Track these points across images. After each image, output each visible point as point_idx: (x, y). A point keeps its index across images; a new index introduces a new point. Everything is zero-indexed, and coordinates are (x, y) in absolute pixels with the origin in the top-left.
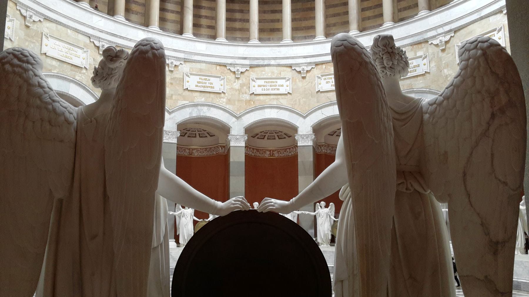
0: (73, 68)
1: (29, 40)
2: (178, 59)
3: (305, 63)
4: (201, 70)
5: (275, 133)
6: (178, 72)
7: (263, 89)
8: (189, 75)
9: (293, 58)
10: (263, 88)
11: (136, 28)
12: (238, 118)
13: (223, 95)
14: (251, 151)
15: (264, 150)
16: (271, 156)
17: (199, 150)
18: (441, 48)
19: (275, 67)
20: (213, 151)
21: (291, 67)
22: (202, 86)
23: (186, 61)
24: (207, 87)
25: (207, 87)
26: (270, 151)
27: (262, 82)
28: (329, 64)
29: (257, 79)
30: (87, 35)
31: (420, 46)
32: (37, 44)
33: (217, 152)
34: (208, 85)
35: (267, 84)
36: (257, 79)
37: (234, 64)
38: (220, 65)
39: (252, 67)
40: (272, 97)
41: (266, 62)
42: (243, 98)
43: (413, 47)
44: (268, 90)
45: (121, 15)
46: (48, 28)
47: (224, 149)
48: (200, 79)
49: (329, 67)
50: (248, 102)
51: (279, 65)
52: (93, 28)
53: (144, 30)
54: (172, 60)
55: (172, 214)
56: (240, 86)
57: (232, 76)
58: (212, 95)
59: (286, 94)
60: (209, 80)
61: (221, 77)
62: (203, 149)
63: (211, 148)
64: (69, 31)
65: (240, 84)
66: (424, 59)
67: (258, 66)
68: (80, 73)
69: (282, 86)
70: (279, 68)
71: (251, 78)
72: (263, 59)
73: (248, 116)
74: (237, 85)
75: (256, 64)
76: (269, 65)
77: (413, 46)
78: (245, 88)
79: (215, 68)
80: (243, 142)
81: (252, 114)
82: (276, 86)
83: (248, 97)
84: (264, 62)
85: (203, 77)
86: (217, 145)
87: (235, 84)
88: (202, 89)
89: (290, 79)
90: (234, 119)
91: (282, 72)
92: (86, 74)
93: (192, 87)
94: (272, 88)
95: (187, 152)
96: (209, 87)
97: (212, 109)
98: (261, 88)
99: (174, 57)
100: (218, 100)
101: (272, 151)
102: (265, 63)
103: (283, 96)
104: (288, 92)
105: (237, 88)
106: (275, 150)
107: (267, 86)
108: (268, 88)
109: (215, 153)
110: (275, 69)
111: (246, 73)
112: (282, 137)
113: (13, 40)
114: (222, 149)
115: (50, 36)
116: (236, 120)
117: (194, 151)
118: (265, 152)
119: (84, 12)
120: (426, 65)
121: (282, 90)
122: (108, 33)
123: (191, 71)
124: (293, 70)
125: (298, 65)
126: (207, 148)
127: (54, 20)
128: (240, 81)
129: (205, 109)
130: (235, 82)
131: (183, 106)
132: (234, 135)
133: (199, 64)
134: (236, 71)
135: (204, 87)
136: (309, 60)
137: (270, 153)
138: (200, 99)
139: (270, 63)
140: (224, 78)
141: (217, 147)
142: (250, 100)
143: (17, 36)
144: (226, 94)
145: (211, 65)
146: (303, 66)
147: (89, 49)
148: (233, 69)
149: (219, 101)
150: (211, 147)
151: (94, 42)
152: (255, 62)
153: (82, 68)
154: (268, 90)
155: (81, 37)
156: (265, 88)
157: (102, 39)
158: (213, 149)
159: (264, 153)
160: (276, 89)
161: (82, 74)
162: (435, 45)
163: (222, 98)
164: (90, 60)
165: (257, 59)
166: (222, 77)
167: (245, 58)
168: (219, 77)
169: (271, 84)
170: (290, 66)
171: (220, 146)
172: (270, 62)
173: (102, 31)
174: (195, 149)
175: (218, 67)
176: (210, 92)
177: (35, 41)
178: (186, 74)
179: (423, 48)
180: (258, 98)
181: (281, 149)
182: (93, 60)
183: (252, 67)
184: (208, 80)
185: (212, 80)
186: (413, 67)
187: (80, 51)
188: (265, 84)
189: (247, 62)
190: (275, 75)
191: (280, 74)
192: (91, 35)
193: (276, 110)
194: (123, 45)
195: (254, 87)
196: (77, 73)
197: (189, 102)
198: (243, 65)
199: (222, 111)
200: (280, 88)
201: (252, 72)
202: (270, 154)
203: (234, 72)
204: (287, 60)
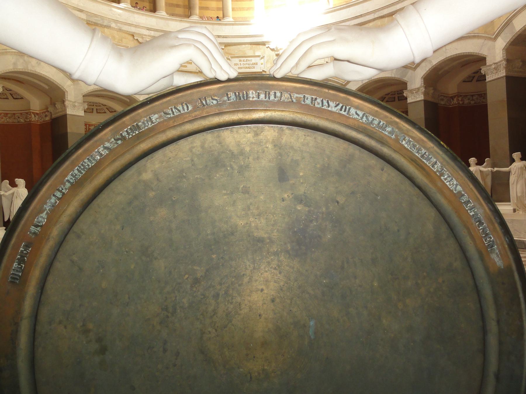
18: (276, 53)
20: (19, 118)
21: (133, 36)
31: (258, 46)
41: (105, 23)
43: (252, 47)
47: (37, 117)
51: (120, 30)
63: (14, 114)
66: (261, 58)
72: (102, 18)
75: (94, 21)
76: (108, 27)
77: (252, 45)
80: (82, 111)
90: (69, 82)
91: (123, 40)
101: (87, 125)
102: (105, 24)
109: (22, 120)
112: (101, 112)
114: (35, 116)
120: (263, 65)
126: (7, 114)
139: (111, 25)
141: (27, 113)
152: (93, 19)
158: (19, 116)
162: (271, 49)
167: (81, 11)
171: (33, 113)
172: (110, 24)
179: (260, 49)
186: (252, 64)
190: (116, 40)
204: (129, 27)
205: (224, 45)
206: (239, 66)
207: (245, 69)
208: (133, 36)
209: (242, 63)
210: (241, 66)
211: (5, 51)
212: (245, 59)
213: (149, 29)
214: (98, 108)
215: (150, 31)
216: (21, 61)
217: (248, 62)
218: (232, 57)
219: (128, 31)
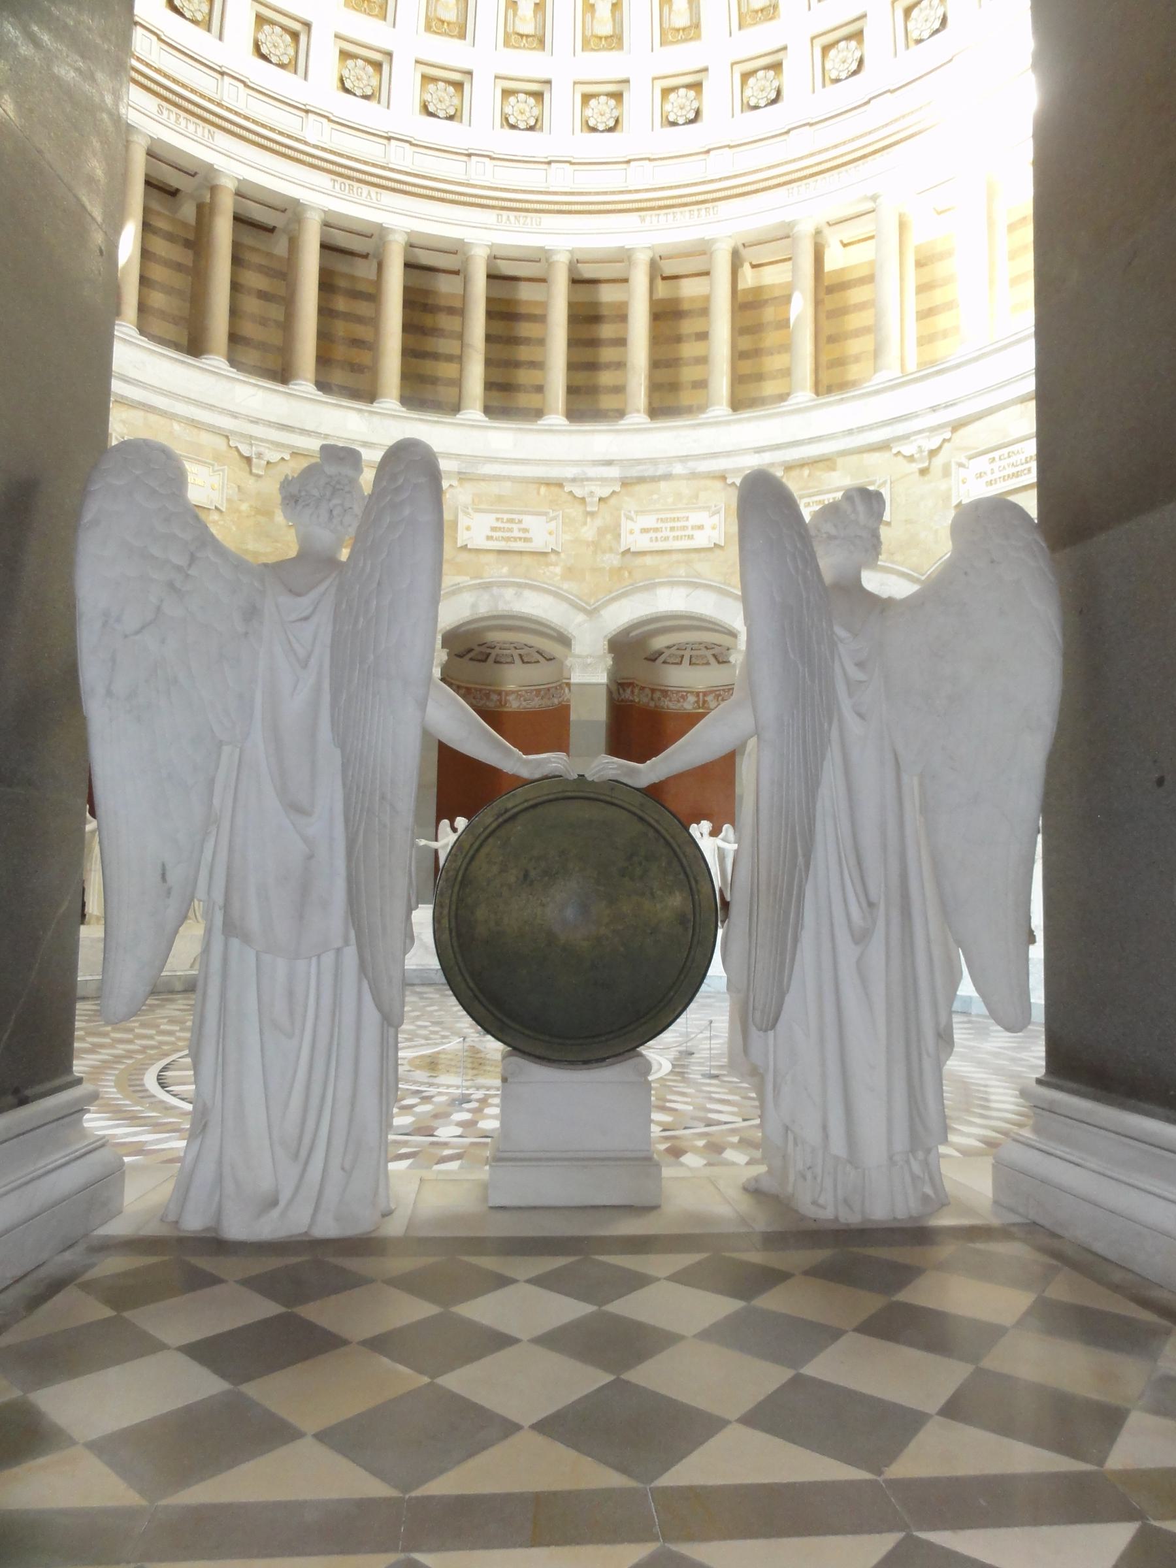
4: (500, 499)
5: (704, 649)
7: (654, 539)
10: (653, 535)
11: (341, 406)
12: (592, 613)
13: (553, 557)
14: (647, 695)
15: (682, 691)
16: (699, 708)
17: (521, 696)
21: (724, 478)
22: (502, 537)
24: (515, 539)
25: (515, 539)
26: (698, 694)
27: (649, 521)
28: (821, 465)
30: (221, 432)
33: (561, 699)
34: (516, 534)
37: (582, 480)
38: (548, 483)
39: (625, 483)
40: (675, 557)
44: (666, 539)
45: (306, 380)
46: (124, 422)
48: (498, 519)
49: (818, 473)
50: (616, 572)
51: (694, 476)
52: (234, 415)
53: (360, 410)
55: (425, 846)
57: (575, 511)
58: (527, 560)
59: (710, 549)
61: (548, 513)
62: (532, 691)
63: (548, 689)
64: (176, 426)
67: (641, 480)
69: (701, 527)
71: (622, 512)
72: (654, 462)
73: (614, 607)
75: (636, 475)
76: (667, 477)
78: (609, 537)
81: (624, 602)
82: (684, 528)
83: (615, 560)
85: (506, 517)
86: (558, 683)
87: (584, 529)
88: (501, 545)
89: (721, 508)
90: (581, 617)
93: (479, 541)
94: (675, 534)
95: (495, 699)
96: (520, 539)
97: (527, 593)
98: (647, 536)
100: (541, 571)
101: (701, 695)
102: (659, 473)
103: (703, 555)
104: (715, 544)
105: (590, 539)
106: (711, 692)
107: (664, 529)
108: (664, 534)
111: (613, 501)
116: (588, 619)
117: (511, 698)
118: (684, 698)
119: (212, 379)
121: (702, 540)
122: (270, 424)
126: (538, 691)
127: (140, 403)
128: (598, 522)
129: (509, 593)
130: (585, 523)
131: (454, 587)
132: (579, 657)
135: (508, 539)
137: (696, 699)
138: (499, 570)
140: (558, 516)
141: (560, 685)
142: (620, 569)
144: (563, 556)
147: (224, 465)
148: (579, 492)
149: (544, 573)
150: (549, 686)
151: (239, 447)
152: (634, 472)
153: (209, 509)
154: (666, 539)
155: (205, 438)
156: (659, 535)
157: (256, 439)
159: (682, 700)
160: (685, 536)
163: (551, 565)
165: (639, 462)
166: (552, 514)
167: (609, 463)
168: (546, 514)
169: (672, 524)
172: (670, 469)
173: (256, 421)
174: (513, 692)
175: (543, 490)
176: (521, 553)
180: (639, 561)
181: (723, 690)
182: (237, 489)
184: (517, 521)
185: (528, 521)
186: (1023, 461)
188: (659, 525)
189: (614, 472)
191: (697, 497)
192: (232, 432)
193: (681, 591)
194: (308, 450)
195: (631, 532)
197: (471, 578)
198: (604, 480)
199: (550, 599)
200: (696, 533)
202: (697, 702)
205: (950, 429)
206: (989, 477)
207: (1004, 480)
208: (724, 478)
209: (995, 466)
210: (993, 477)
211: (457, 586)
212: (1005, 451)
214: (694, 653)
215: (763, 454)
216: (486, 597)
217: (1013, 460)
218: (970, 458)
219: (709, 472)
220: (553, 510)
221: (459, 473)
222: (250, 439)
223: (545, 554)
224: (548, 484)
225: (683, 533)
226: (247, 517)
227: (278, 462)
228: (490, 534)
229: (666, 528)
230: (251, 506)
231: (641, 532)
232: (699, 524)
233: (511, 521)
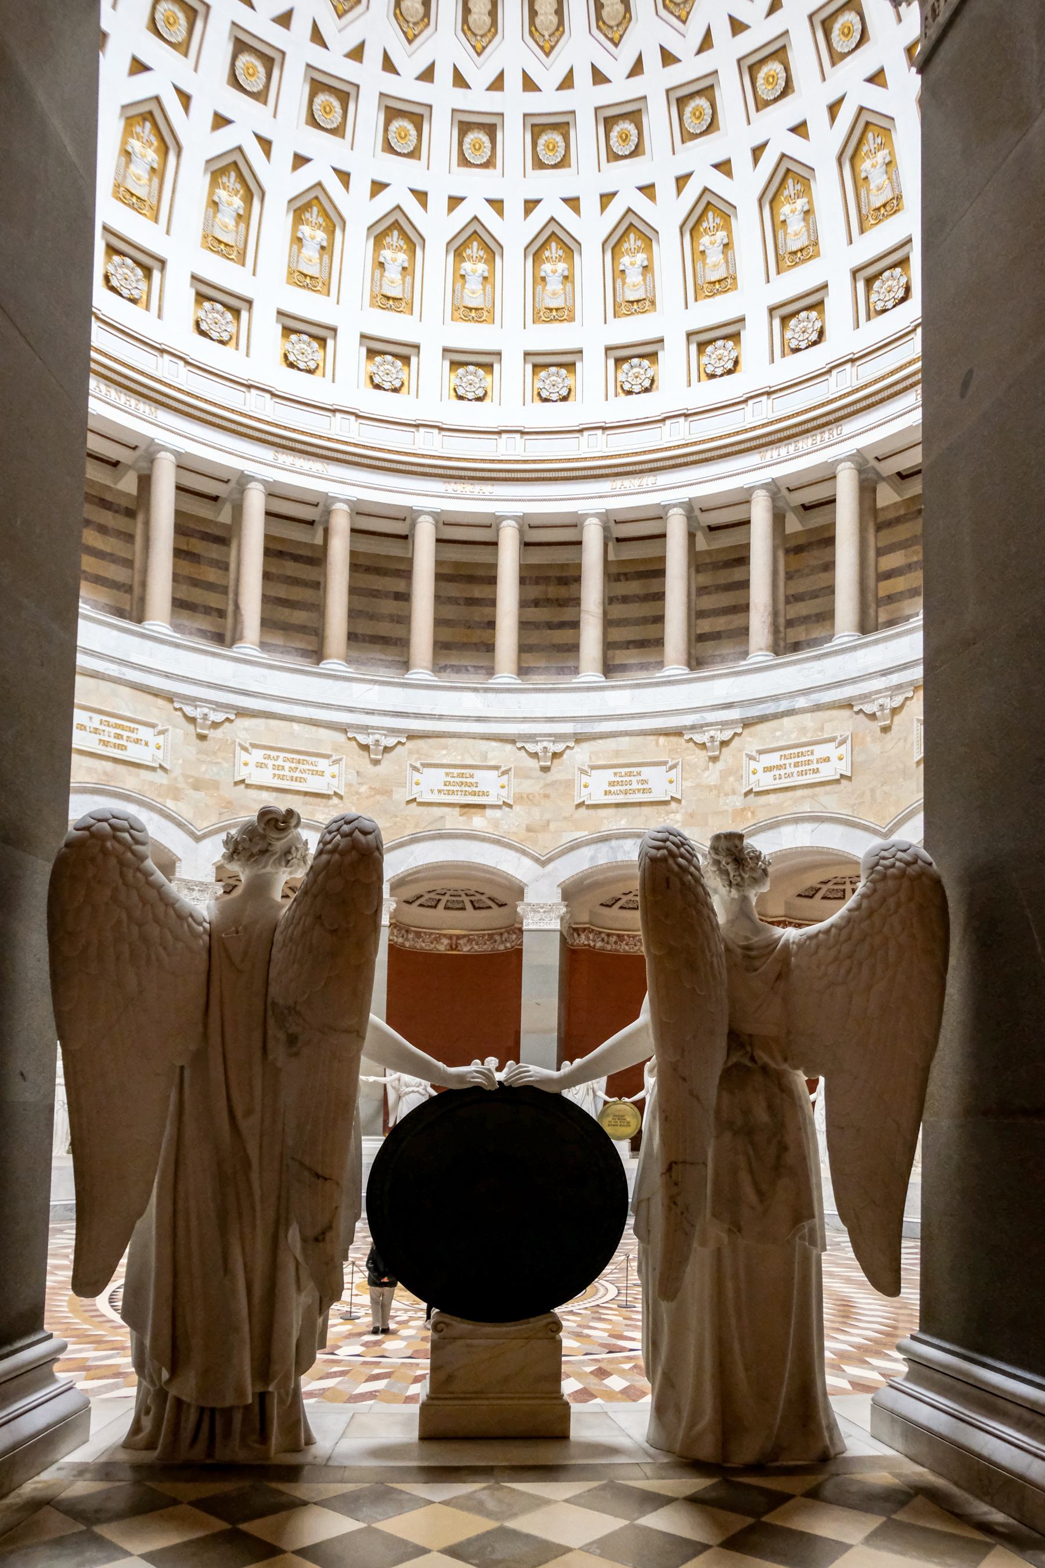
0: (308, 799)
1: (209, 759)
2: (558, 737)
3: (886, 689)
4: (617, 753)
6: (560, 767)
8: (589, 770)
9: (853, 681)
19: (809, 715)
21: (851, 706)
22: (620, 791)
23: (579, 738)
27: (773, 759)
29: (761, 752)
32: (225, 765)
34: (635, 786)
35: (787, 762)
36: (761, 752)
37: (702, 726)
38: (666, 733)
39: (747, 723)
41: (784, 705)
42: (727, 805)
48: (615, 774)
51: (818, 708)
54: (545, 744)
56: (721, 777)
60: (639, 774)
65: (720, 771)
68: (325, 806)
70: (820, 713)
74: (712, 775)
76: (790, 713)
78: (731, 779)
79: (654, 743)
84: (778, 707)
85: (624, 770)
87: (707, 773)
88: (621, 799)
91: (826, 725)
92: (341, 805)
96: (639, 790)
99: (550, 735)
105: (712, 783)
107: (788, 766)
110: (807, 719)
113: (167, 767)
115: (251, 744)
123: (593, 758)
124: (857, 713)
125: (866, 697)
128: (720, 765)
130: (707, 768)
133: (614, 739)
134: (706, 741)
136: (895, 679)
143: (178, 759)
145: (643, 737)
146: (880, 698)
148: (699, 738)
161: (331, 808)
164: (350, 777)
168: (665, 763)
170: (847, 705)
175: (662, 740)
176: (640, 804)
177: (220, 760)
178: (579, 769)
183: (747, 723)
184: (635, 773)
187: (323, 764)
188: (783, 762)
190: (809, 735)
191: (822, 729)
196: (319, 806)
201: (751, 737)
203: (703, 746)
204: (839, 690)
213: (885, 673)
215: (889, 676)
220: (673, 759)
221: (575, 734)
222: (365, 729)
223: (665, 803)
224: (667, 734)
225: (807, 767)
226: (367, 798)
227: (396, 746)
228: (608, 789)
229: (790, 764)
230: (370, 788)
231: (764, 772)
232: (825, 756)
233: (630, 774)
